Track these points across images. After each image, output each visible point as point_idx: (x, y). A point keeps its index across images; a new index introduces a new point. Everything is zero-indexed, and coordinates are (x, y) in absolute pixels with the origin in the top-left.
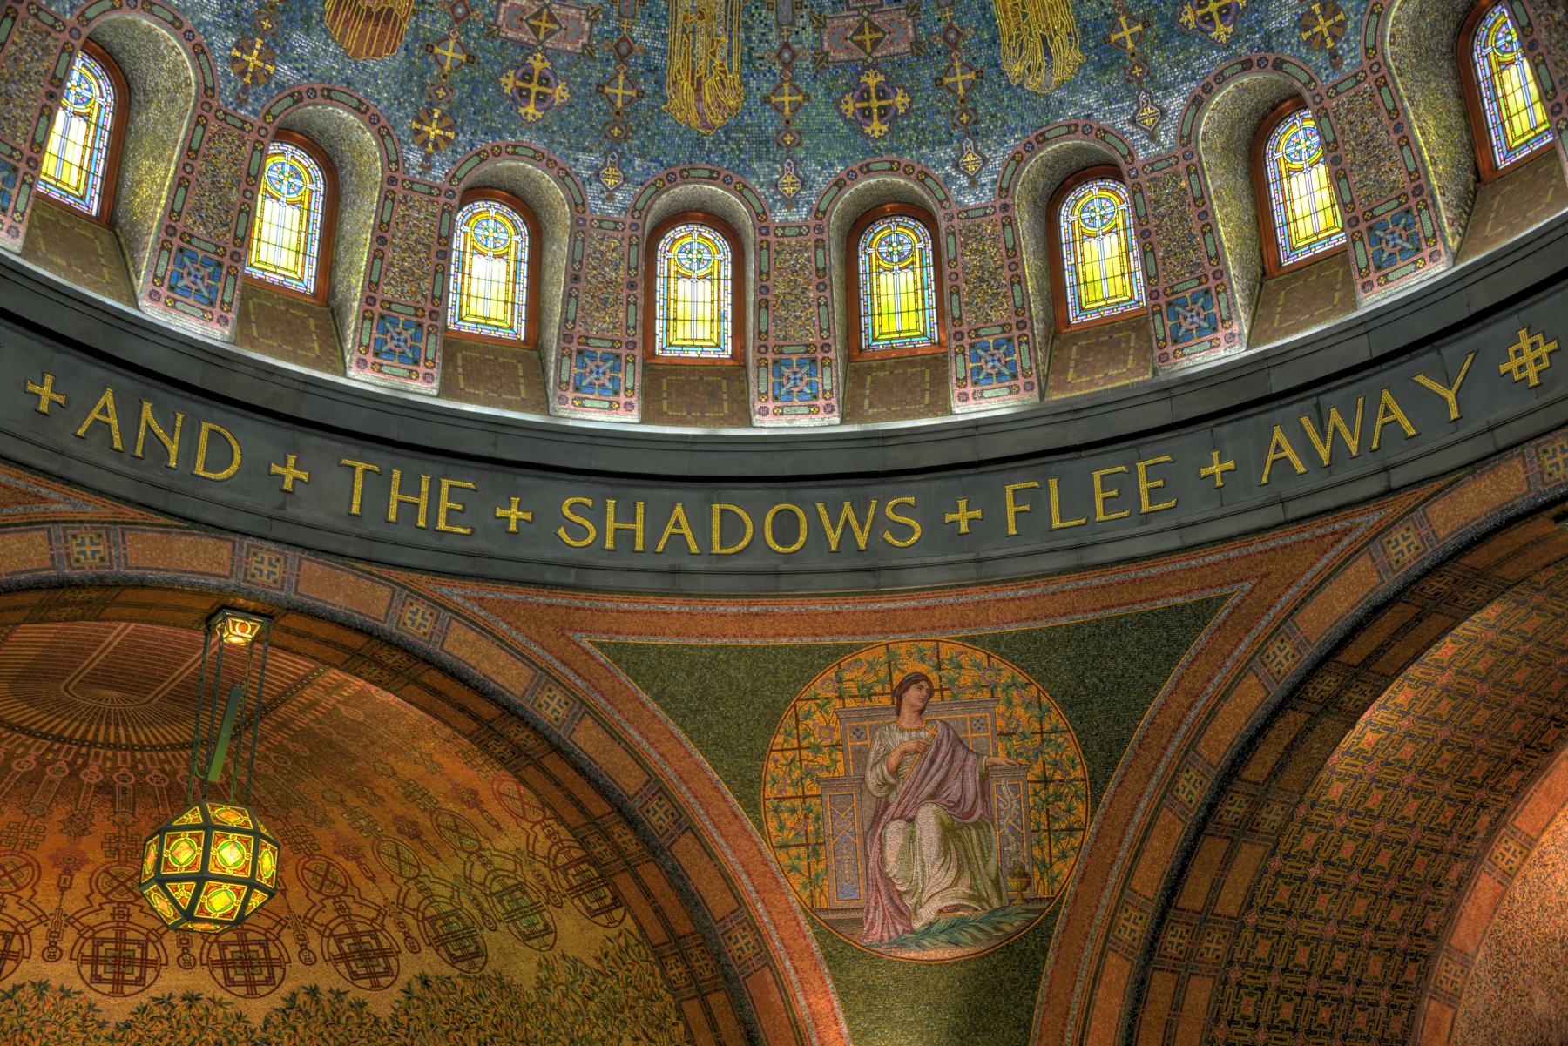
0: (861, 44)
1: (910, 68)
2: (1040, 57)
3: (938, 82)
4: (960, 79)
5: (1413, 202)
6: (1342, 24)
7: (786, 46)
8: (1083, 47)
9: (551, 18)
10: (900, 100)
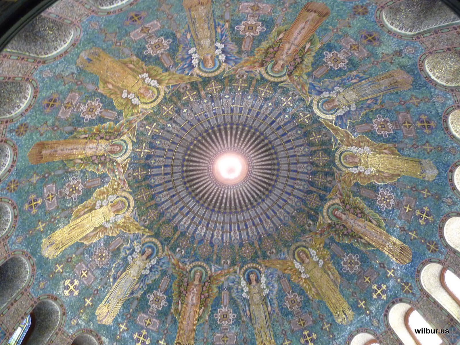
0: (301, 325)
1: (314, 327)
2: (344, 316)
3: (322, 329)
4: (326, 326)
5: (452, 323)
6: (411, 286)
7: (283, 330)
8: (353, 310)
9: (227, 337)
10: (314, 336)
